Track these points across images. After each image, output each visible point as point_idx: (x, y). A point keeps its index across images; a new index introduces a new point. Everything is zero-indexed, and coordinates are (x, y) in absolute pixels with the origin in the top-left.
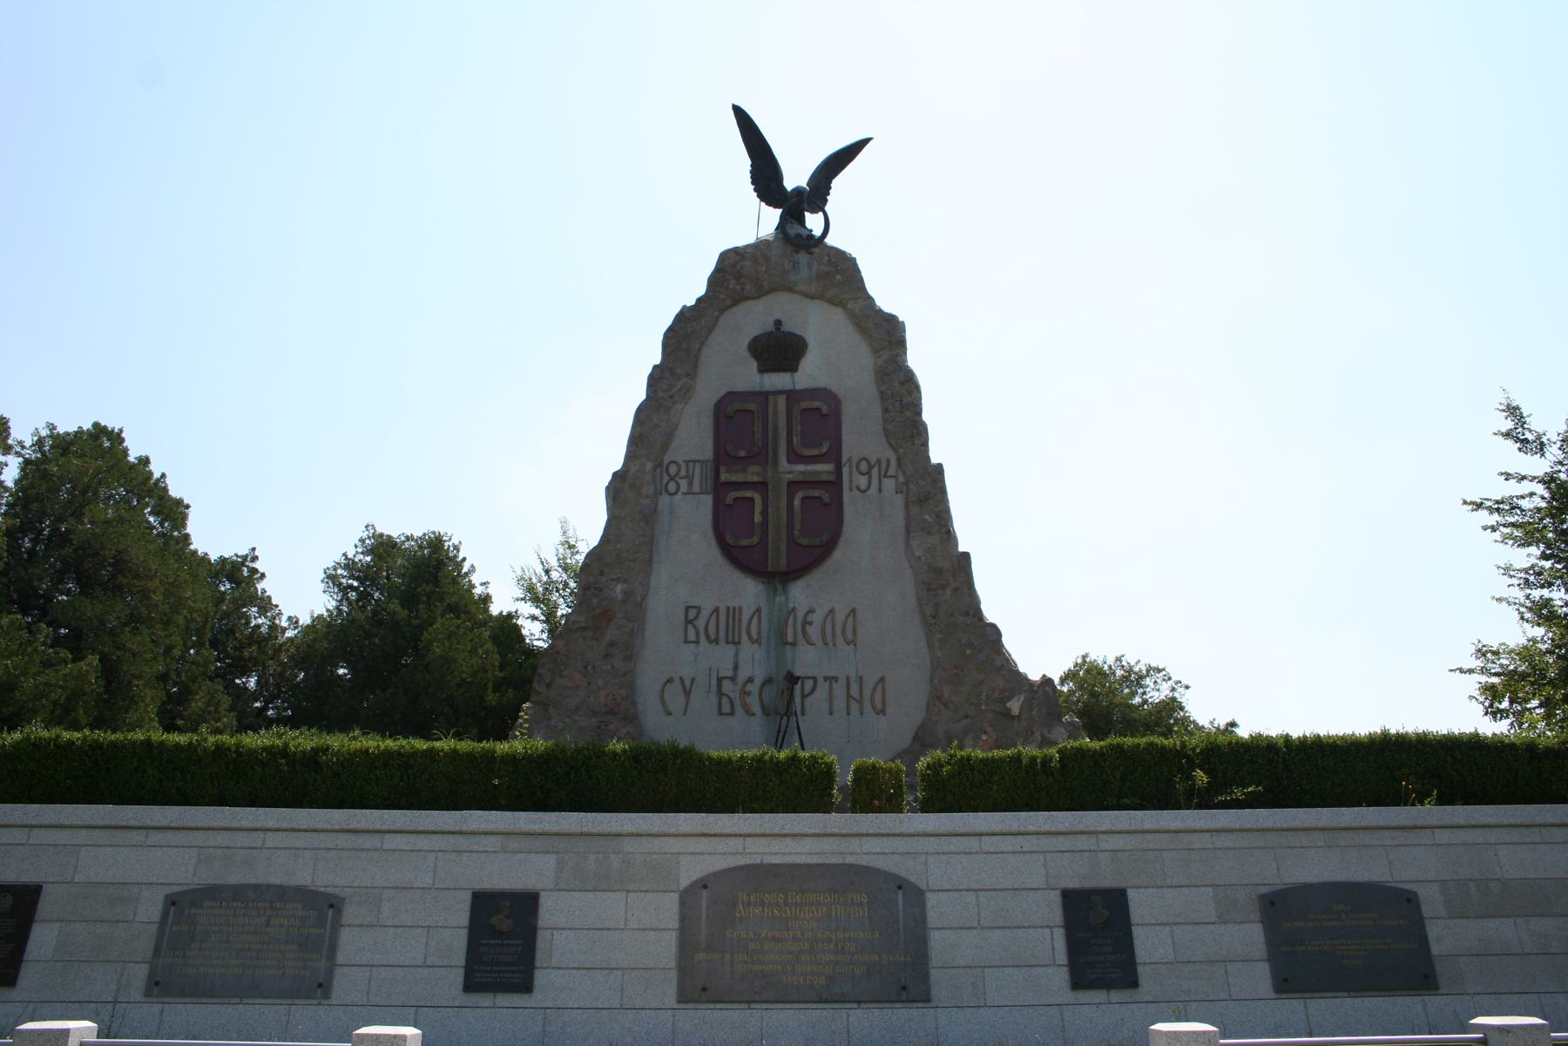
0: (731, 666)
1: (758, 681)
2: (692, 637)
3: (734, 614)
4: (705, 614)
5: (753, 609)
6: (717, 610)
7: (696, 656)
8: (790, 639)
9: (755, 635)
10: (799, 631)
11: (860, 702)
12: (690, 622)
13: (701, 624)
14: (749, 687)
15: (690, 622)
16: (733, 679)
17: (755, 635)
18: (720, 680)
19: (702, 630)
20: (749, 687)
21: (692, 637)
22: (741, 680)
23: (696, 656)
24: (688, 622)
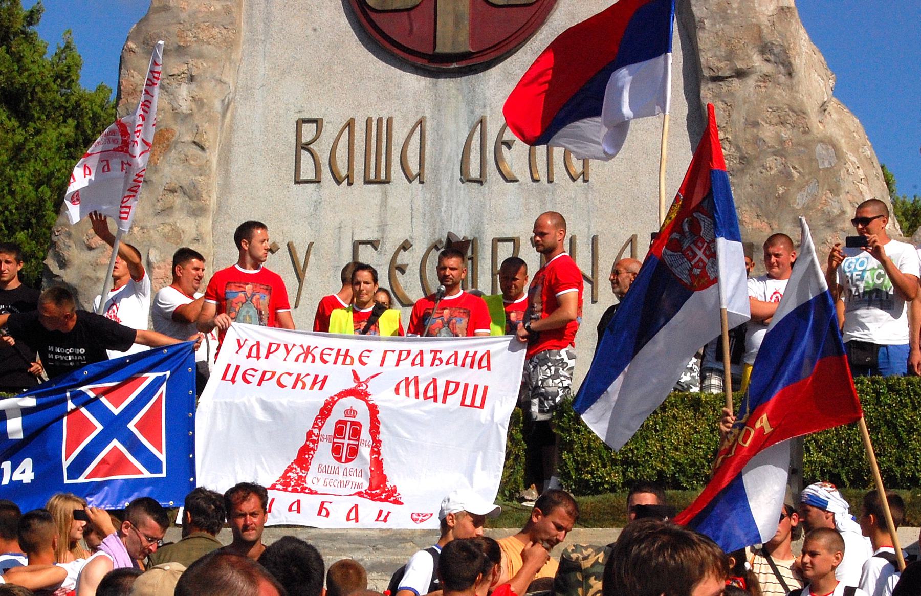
0: (374, 222)
1: (419, 248)
2: (308, 171)
3: (381, 129)
4: (330, 131)
5: (413, 121)
6: (350, 124)
7: (317, 204)
8: (475, 173)
9: (414, 168)
10: (490, 156)
11: (593, 282)
12: (306, 147)
13: (322, 149)
14: (404, 258)
15: (306, 147)
16: (374, 244)
17: (414, 168)
18: (356, 245)
19: (324, 160)
20: (404, 258)
21: (308, 171)
22: (390, 247)
23: (317, 204)
24: (303, 146)
